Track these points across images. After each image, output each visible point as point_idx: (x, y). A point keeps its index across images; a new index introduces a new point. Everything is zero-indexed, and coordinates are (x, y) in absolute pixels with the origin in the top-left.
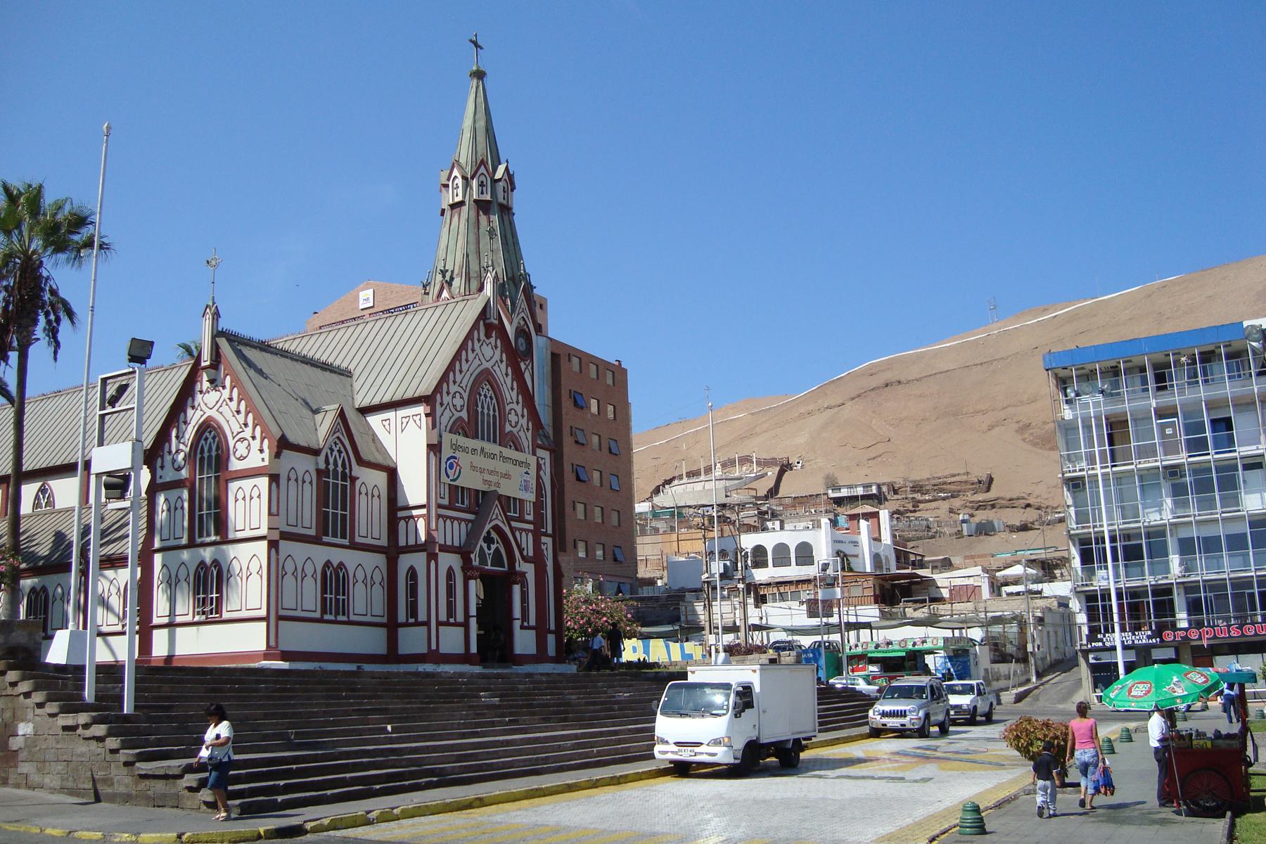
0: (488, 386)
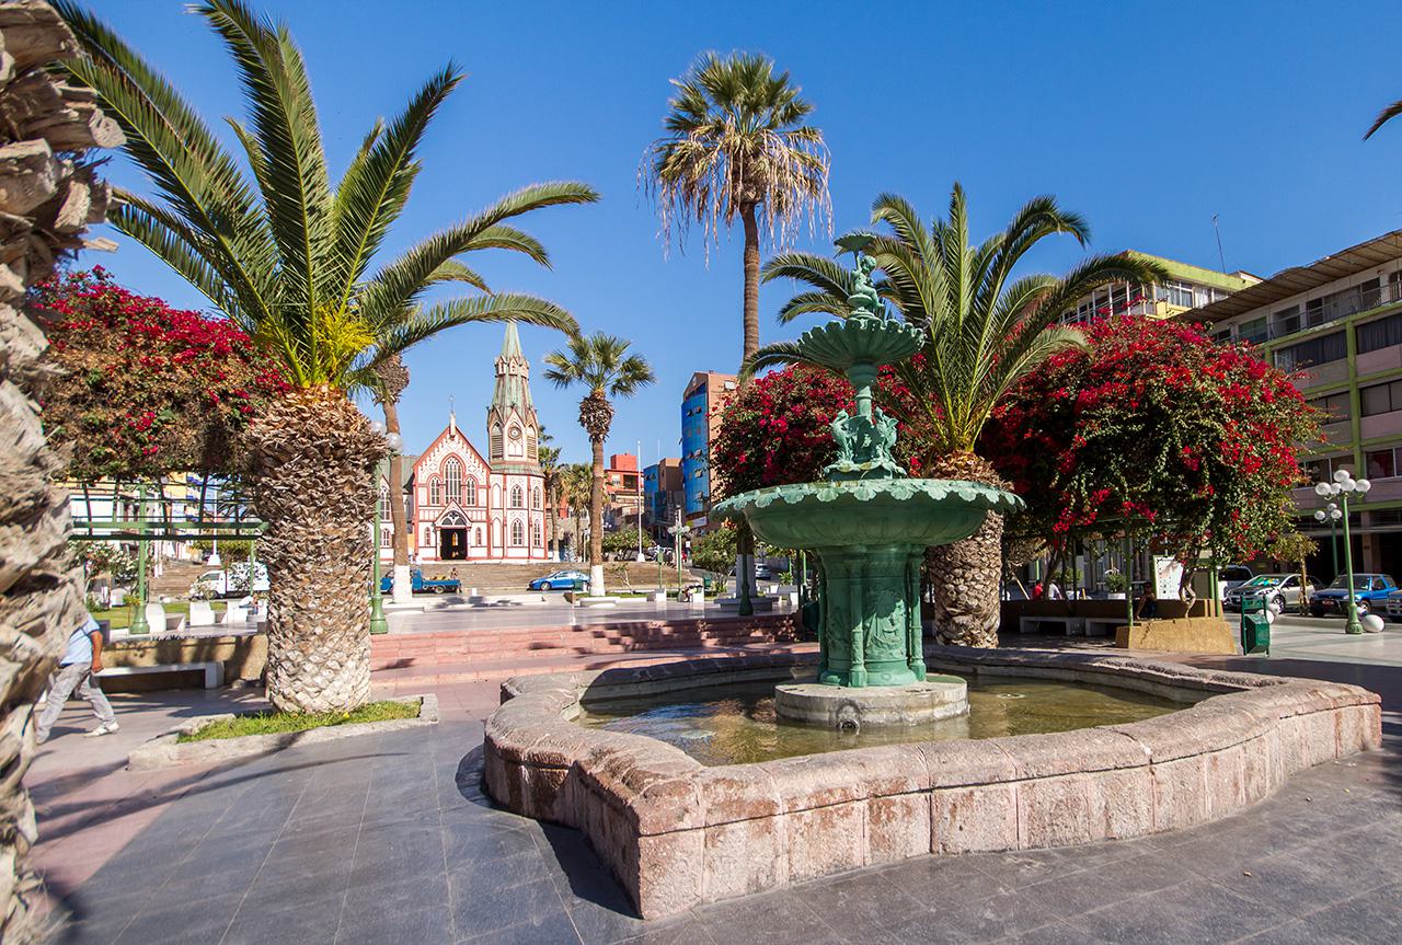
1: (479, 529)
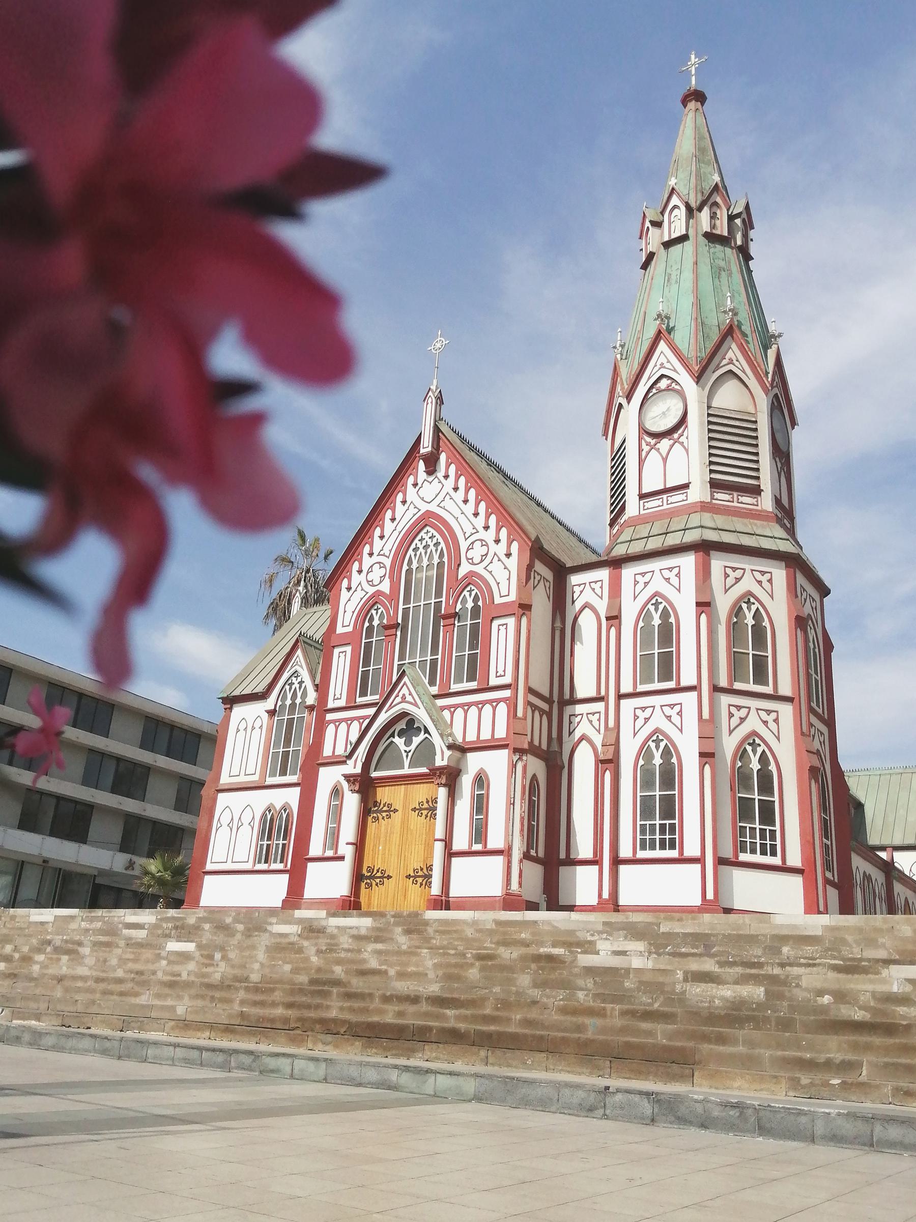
1: (481, 780)
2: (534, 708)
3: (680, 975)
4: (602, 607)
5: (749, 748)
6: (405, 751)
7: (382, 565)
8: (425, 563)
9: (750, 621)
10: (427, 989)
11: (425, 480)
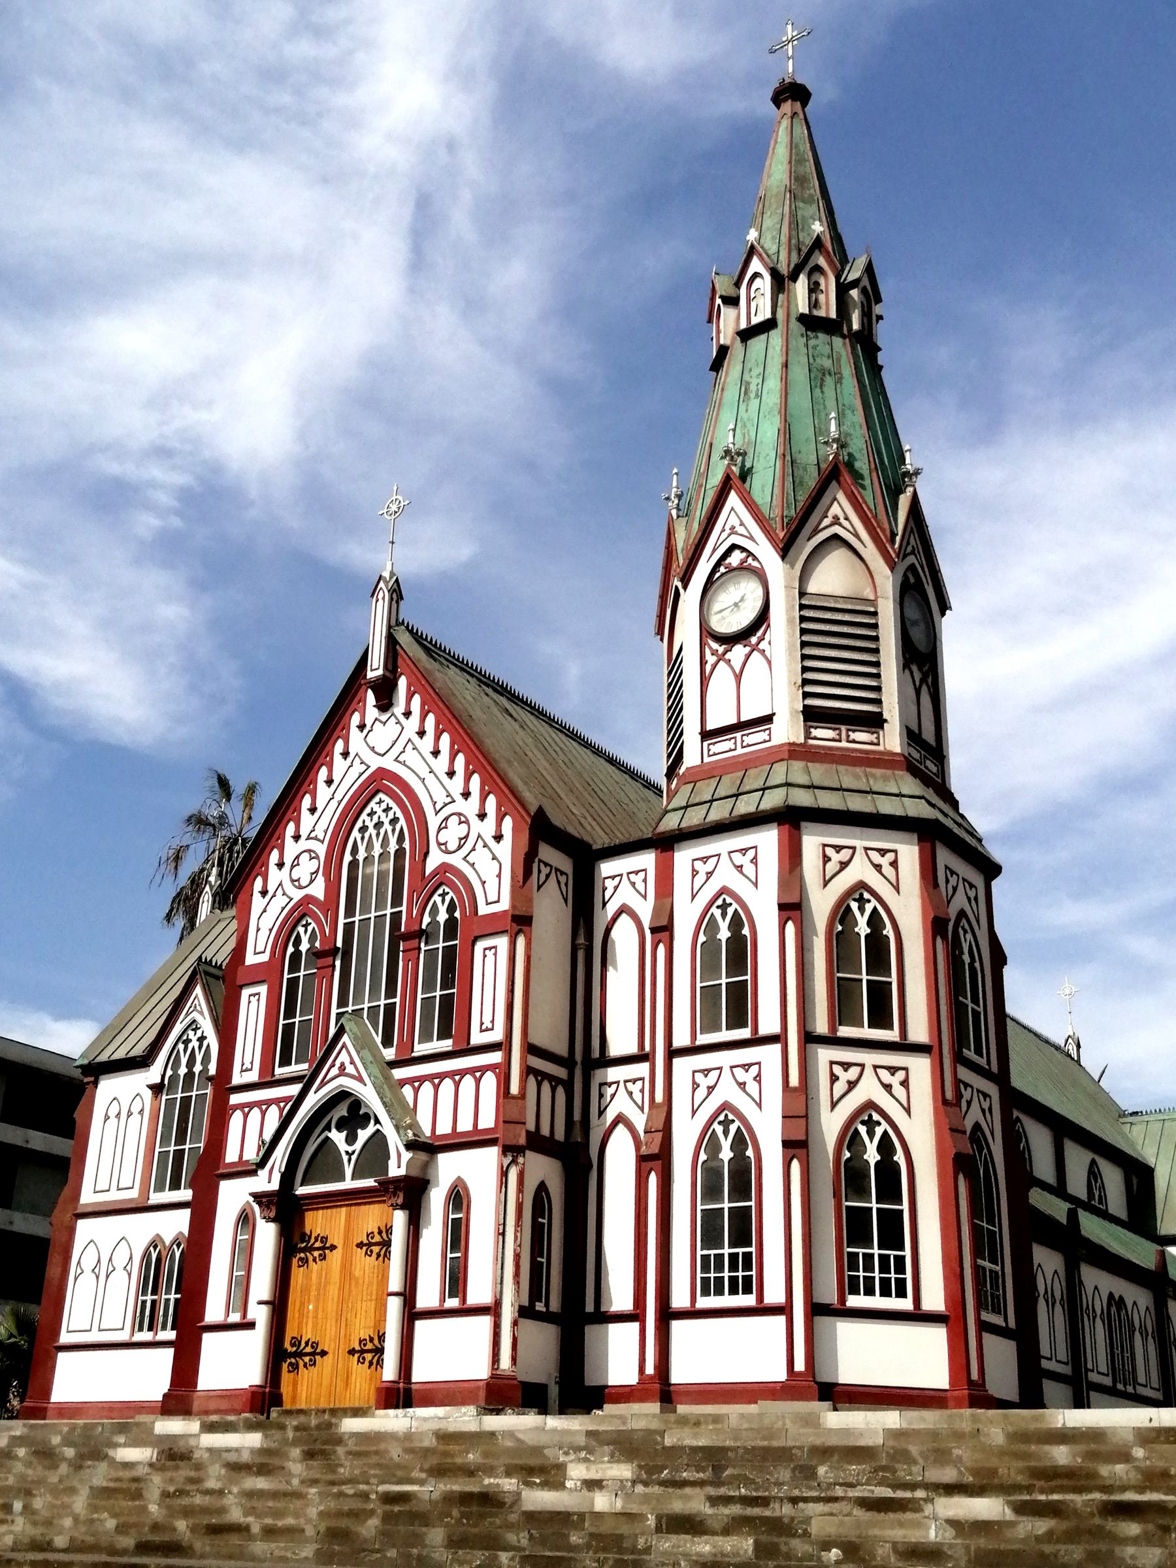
0: (388, 800)
1: (458, 1197)
2: (540, 1076)
3: (651, 1521)
4: (645, 910)
5: (863, 1130)
6: (347, 1153)
7: (313, 855)
8: (377, 850)
9: (863, 929)
10: (297, 1555)
11: (376, 719)
